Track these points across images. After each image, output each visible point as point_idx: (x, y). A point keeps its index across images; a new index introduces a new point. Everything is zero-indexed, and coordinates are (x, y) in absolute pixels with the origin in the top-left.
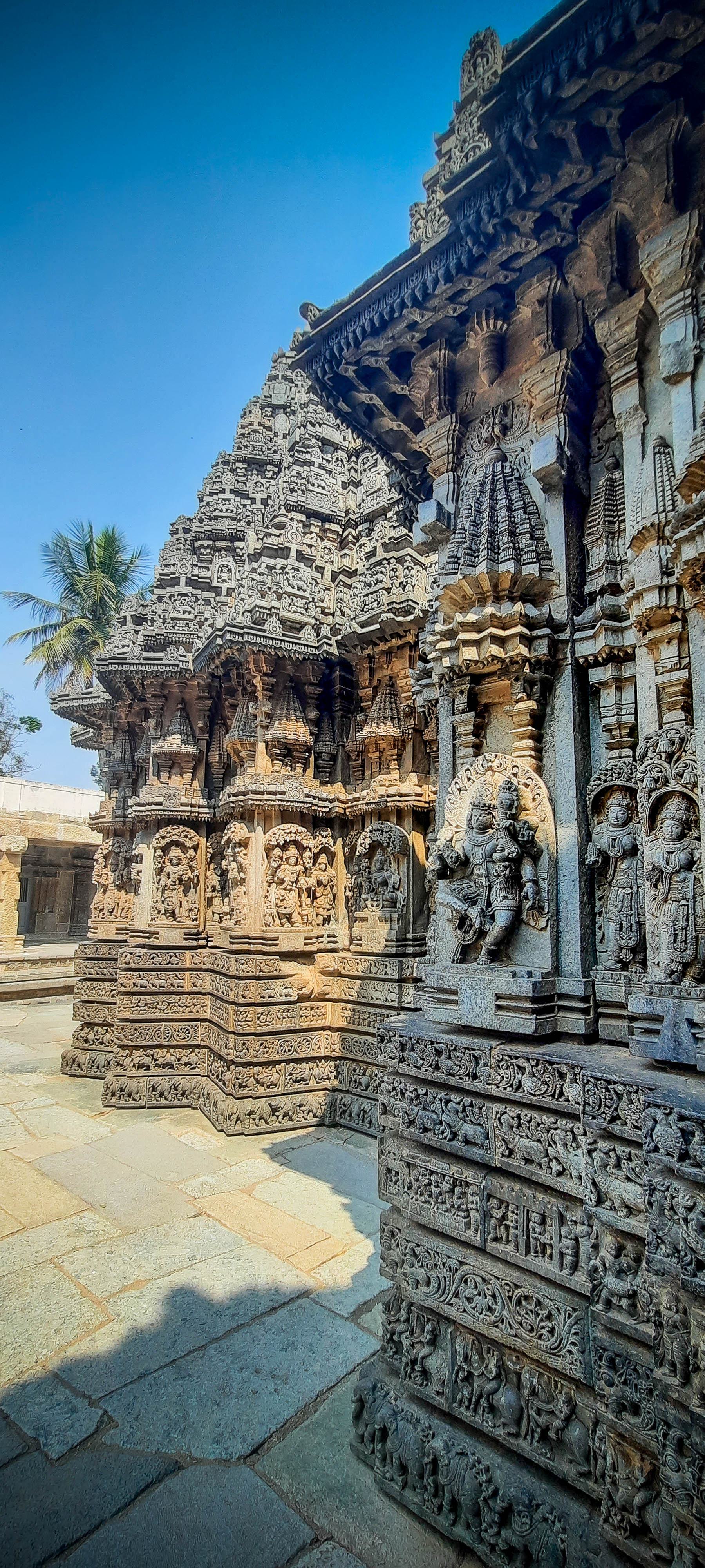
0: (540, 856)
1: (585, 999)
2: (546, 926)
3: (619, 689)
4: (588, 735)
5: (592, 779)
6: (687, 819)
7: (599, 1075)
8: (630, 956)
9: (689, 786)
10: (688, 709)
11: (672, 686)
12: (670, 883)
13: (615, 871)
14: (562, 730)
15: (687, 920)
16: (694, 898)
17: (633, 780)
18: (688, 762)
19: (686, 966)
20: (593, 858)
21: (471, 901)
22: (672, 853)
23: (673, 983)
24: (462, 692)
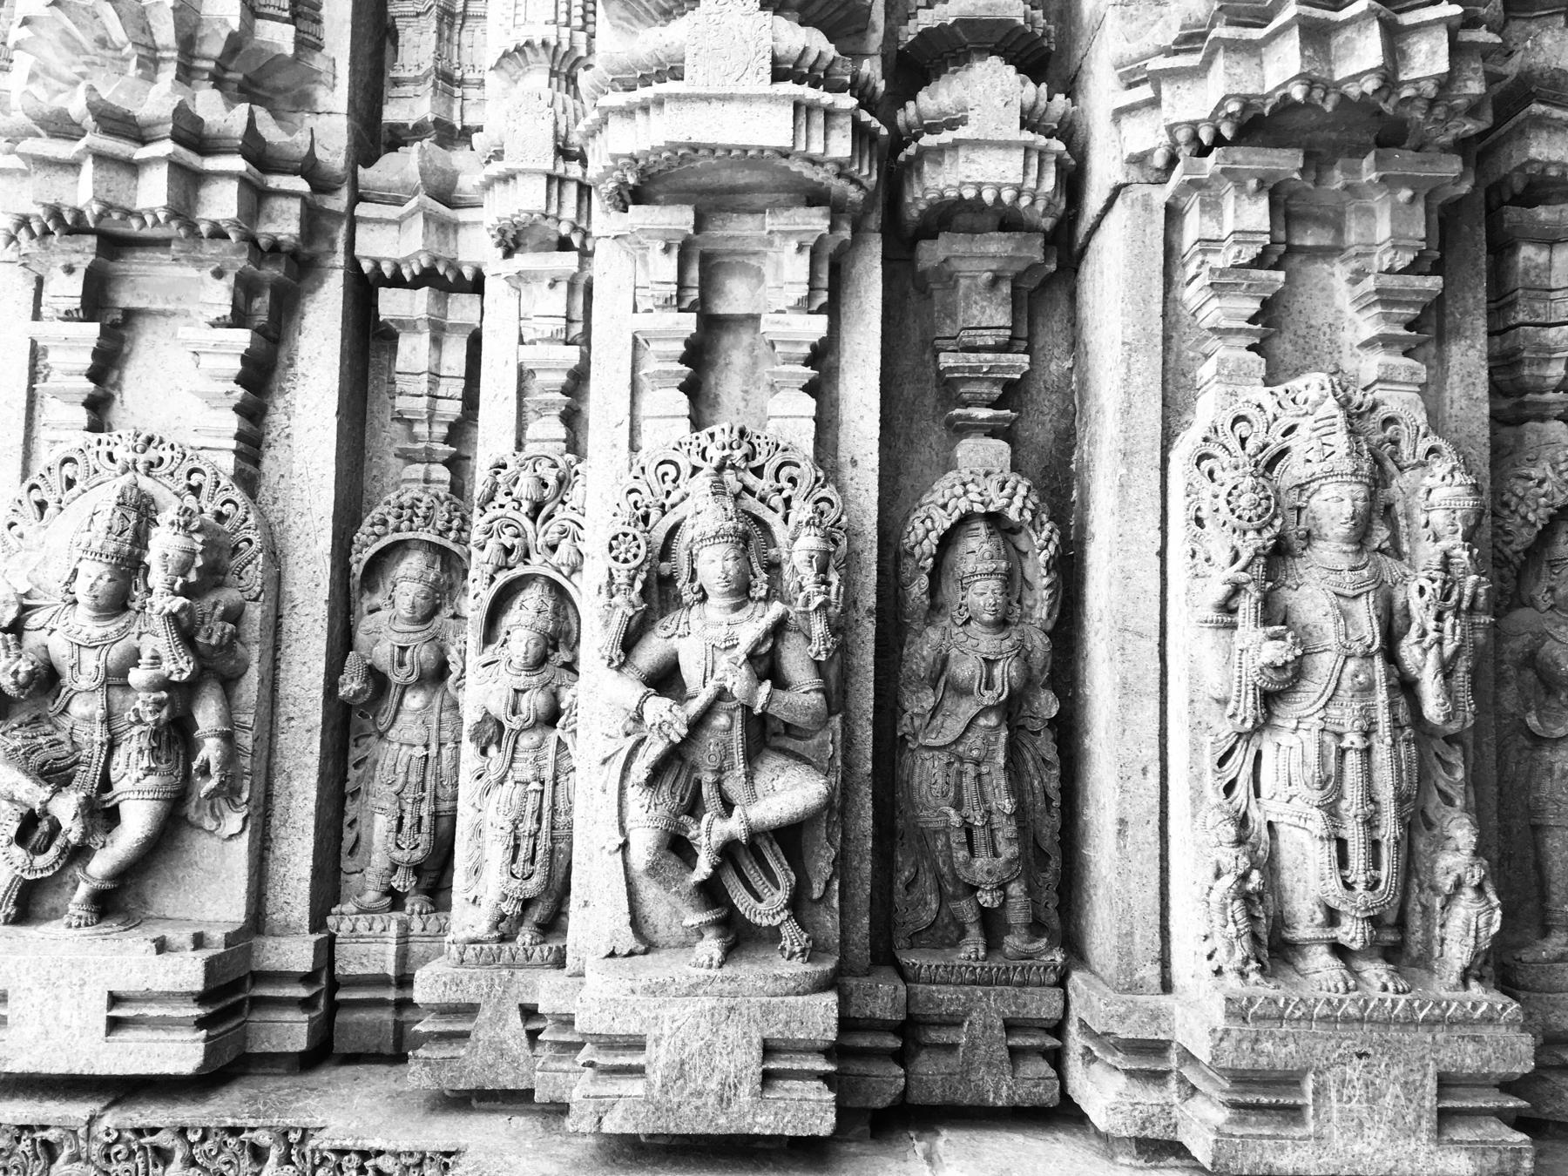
0: (241, 676)
1: (307, 979)
2: (242, 831)
3: (437, 342)
4: (363, 422)
5: (368, 520)
6: (555, 629)
7: (348, 1143)
8: (412, 880)
9: (565, 570)
10: (572, 418)
11: (549, 370)
12: (514, 750)
13: (397, 712)
14: (310, 404)
15: (539, 820)
16: (556, 778)
17: (452, 535)
18: (567, 524)
19: (527, 904)
20: (355, 686)
21: (56, 775)
22: (524, 691)
23: (502, 939)
24: (70, 270)
